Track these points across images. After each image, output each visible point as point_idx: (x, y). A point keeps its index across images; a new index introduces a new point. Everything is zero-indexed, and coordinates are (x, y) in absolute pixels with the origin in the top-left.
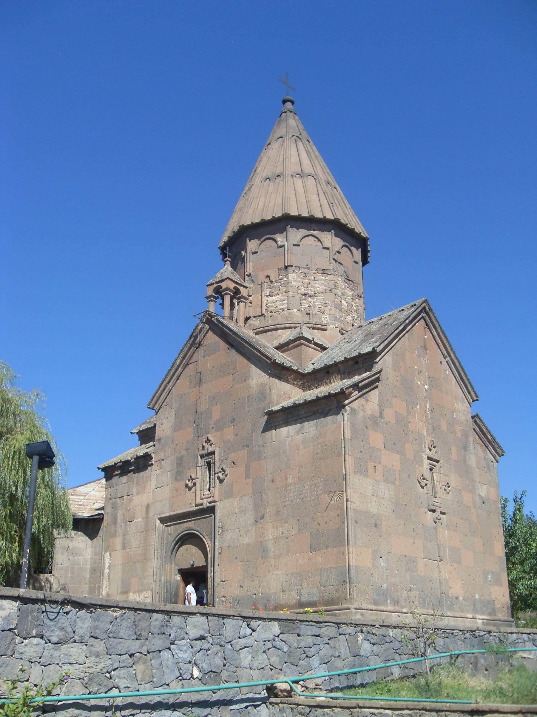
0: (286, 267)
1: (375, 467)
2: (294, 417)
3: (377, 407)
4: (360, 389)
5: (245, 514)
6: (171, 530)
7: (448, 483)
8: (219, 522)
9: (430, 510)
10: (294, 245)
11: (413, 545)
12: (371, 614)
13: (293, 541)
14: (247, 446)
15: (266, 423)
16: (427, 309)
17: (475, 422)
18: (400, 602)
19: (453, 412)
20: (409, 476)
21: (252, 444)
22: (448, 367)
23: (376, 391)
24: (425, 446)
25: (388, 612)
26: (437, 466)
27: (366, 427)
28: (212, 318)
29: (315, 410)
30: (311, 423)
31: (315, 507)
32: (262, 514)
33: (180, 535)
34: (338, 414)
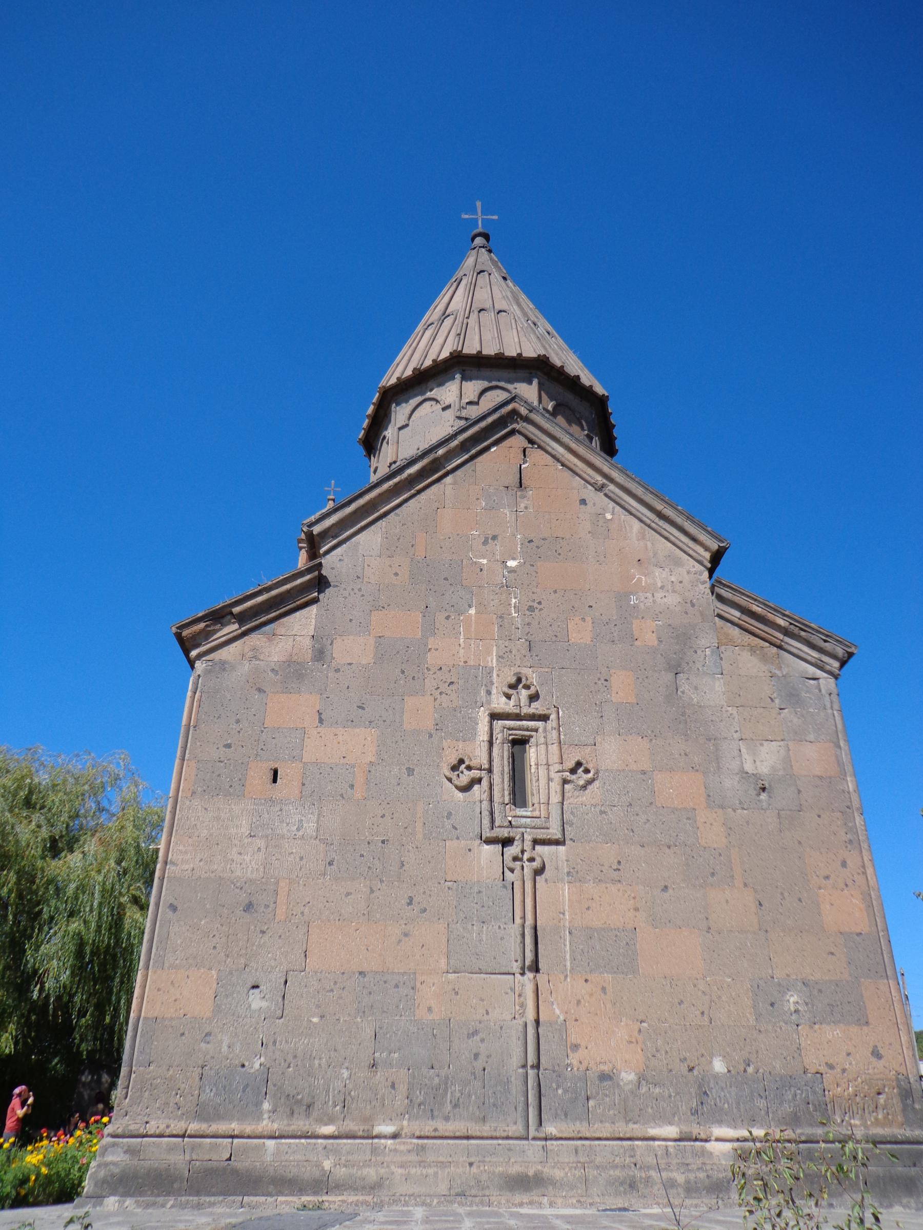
1: (276, 772)
3: (308, 642)
4: (241, 619)
7: (579, 764)
9: (489, 841)
10: (400, 429)
11: (400, 941)
12: (171, 1149)
16: (523, 411)
17: (720, 598)
18: (318, 1105)
19: (622, 597)
20: (410, 771)
22: (612, 504)
23: (313, 609)
24: (489, 693)
25: (249, 1137)
26: (540, 730)
27: (260, 690)
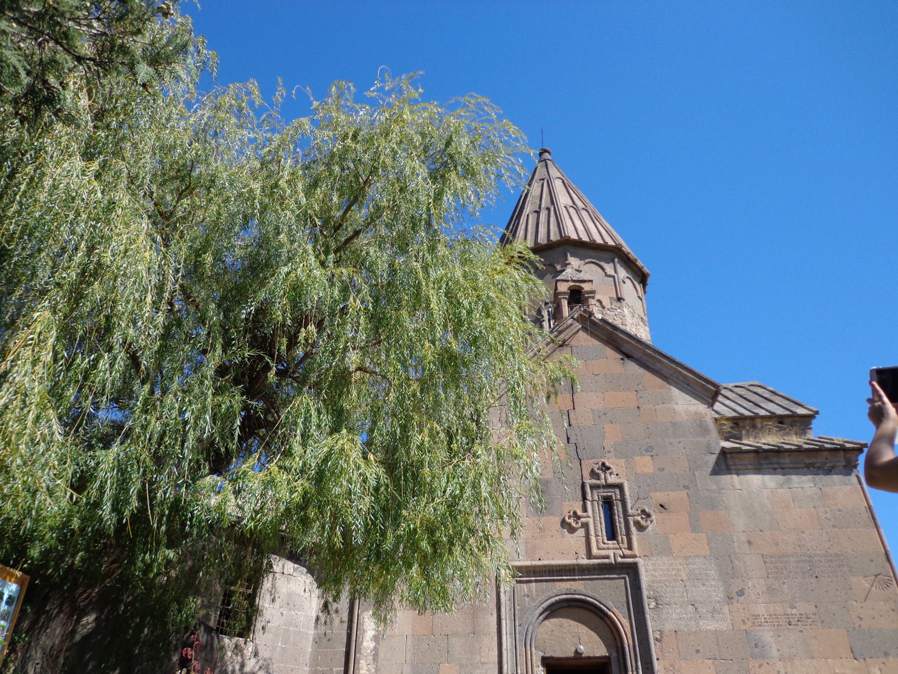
0: (619, 299)
2: (770, 464)
5: (704, 585)
6: (530, 590)
8: (649, 590)
13: (815, 638)
14: (685, 487)
15: (717, 463)
21: (696, 486)
28: (590, 316)
29: (808, 462)
30: (804, 478)
31: (843, 592)
32: (740, 589)
33: (553, 600)
34: (849, 474)
